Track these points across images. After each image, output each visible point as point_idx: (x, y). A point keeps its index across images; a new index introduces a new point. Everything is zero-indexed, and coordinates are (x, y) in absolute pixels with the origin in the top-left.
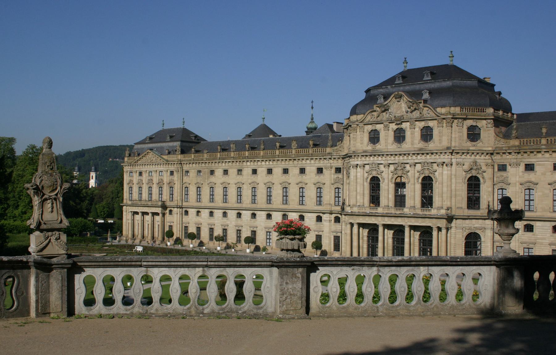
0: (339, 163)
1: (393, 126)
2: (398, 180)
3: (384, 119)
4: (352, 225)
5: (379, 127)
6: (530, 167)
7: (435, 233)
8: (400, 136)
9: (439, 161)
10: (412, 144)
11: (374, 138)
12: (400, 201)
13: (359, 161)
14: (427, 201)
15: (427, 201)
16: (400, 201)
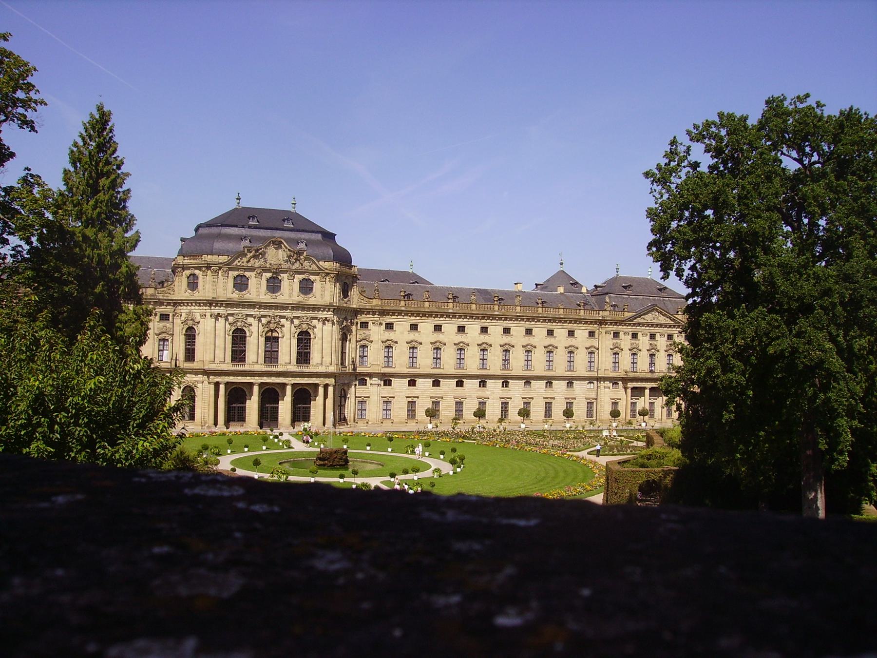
0: (168, 310)
1: (269, 275)
2: (269, 334)
3: (257, 265)
4: (217, 385)
5: (247, 274)
6: (390, 326)
7: (321, 390)
8: (274, 286)
9: (321, 316)
10: (291, 295)
11: (241, 284)
12: (271, 356)
13: (222, 310)
14: (303, 356)
15: (303, 356)
16: (271, 356)
